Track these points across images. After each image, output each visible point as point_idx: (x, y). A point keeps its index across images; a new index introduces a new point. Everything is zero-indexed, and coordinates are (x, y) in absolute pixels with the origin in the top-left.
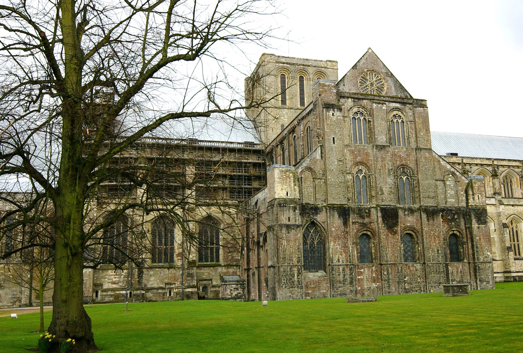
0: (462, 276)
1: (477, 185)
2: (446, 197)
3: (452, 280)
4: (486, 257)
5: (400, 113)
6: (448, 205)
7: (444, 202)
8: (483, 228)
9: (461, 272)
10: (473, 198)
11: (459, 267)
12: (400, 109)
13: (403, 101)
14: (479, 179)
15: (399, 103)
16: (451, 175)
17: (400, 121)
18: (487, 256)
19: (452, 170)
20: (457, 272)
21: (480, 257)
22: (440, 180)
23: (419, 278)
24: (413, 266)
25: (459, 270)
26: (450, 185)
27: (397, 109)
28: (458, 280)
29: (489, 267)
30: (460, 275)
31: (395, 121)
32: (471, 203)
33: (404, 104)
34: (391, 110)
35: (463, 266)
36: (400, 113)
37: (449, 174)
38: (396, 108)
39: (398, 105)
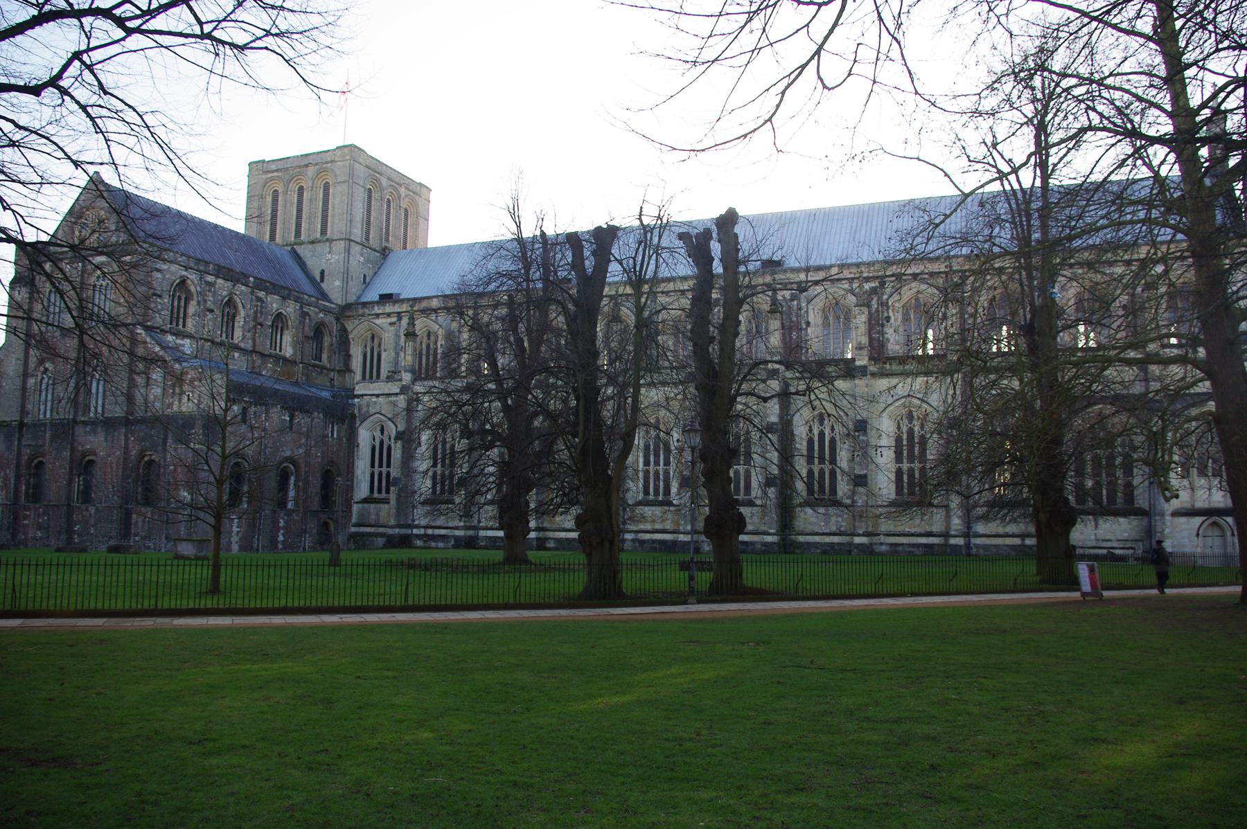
10: (180, 400)
20: (144, 522)
28: (144, 534)
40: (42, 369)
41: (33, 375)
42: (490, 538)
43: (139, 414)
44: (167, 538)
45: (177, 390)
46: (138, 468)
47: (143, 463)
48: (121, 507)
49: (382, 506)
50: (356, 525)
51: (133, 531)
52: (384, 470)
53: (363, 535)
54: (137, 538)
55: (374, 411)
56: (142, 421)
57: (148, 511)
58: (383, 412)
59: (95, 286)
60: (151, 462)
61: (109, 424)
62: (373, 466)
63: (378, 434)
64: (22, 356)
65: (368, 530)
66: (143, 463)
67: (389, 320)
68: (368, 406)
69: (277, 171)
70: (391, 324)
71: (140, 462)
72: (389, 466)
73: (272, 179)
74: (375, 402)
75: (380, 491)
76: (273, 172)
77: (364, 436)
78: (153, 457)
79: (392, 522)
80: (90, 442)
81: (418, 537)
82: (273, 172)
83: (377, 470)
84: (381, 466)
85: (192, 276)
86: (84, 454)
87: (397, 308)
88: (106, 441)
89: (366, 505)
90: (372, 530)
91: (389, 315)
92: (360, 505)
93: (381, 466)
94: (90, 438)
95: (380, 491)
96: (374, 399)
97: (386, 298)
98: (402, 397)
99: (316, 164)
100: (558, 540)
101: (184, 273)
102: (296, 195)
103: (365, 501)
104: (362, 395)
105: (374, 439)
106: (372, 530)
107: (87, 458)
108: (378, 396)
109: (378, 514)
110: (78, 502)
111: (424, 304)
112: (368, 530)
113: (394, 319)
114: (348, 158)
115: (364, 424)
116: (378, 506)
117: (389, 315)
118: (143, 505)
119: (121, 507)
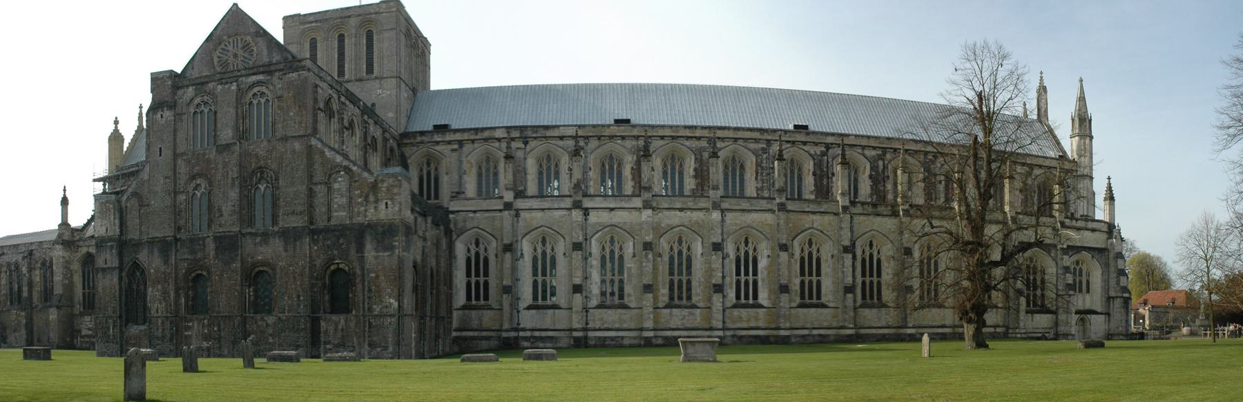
0: (343, 336)
1: (385, 185)
2: (329, 210)
3: (325, 342)
4: (387, 307)
5: (264, 89)
6: (333, 222)
7: (325, 217)
8: (386, 258)
9: (342, 330)
11: (339, 323)
12: (264, 83)
13: (267, 70)
14: (392, 174)
15: (263, 73)
16: (342, 173)
17: (263, 101)
18: (388, 304)
19: (345, 163)
20: (336, 330)
21: (375, 307)
22: (320, 183)
23: (271, 338)
24: (262, 319)
25: (340, 327)
26: (339, 190)
27: (259, 83)
28: (336, 342)
29: (390, 324)
30: (339, 334)
31: (255, 102)
32: (370, 217)
33: (270, 73)
34: (249, 87)
35: (346, 321)
36: (264, 89)
37: (340, 171)
38: (258, 83)
39: (261, 77)
40: (193, 185)
41: (183, 192)
42: (600, 338)
43: (321, 223)
44: (370, 345)
45: (372, 198)
46: (324, 277)
47: (328, 272)
48: (309, 316)
49: (485, 312)
50: (457, 330)
51: (322, 339)
52: (482, 279)
53: (465, 339)
54: (328, 347)
55: (472, 226)
56: (327, 230)
57: (341, 319)
58: (481, 227)
59: (251, 103)
60: (339, 269)
61: (290, 236)
62: (468, 274)
63: (473, 247)
64: (171, 173)
65: (471, 334)
66: (328, 272)
67: (450, 147)
68: (465, 221)
69: (316, 22)
70: (453, 150)
71: (326, 271)
72: (486, 274)
73: (311, 29)
74: (473, 218)
75: (477, 298)
76: (312, 22)
77: (460, 249)
78: (340, 266)
79: (506, 326)
80: (262, 253)
81: (526, 339)
82: (312, 22)
83: (473, 279)
84: (477, 275)
85: (335, 96)
86: (254, 265)
87: (458, 136)
88: (286, 250)
89: (467, 311)
90: (476, 334)
91: (449, 142)
92: (461, 312)
93: (477, 275)
94: (261, 249)
95: (477, 298)
96: (471, 215)
97: (442, 128)
98: (506, 212)
99: (359, 15)
100: (666, 338)
101: (330, 92)
102: (336, 42)
103: (464, 308)
104: (458, 211)
105: (469, 251)
106: (476, 334)
107: (257, 269)
108: (475, 212)
109: (480, 320)
110: (250, 313)
111: (486, 134)
112: (471, 334)
113: (456, 146)
114: (394, 9)
115: (462, 237)
116: (480, 311)
117: (449, 142)
118: (330, 313)
119: (309, 316)
